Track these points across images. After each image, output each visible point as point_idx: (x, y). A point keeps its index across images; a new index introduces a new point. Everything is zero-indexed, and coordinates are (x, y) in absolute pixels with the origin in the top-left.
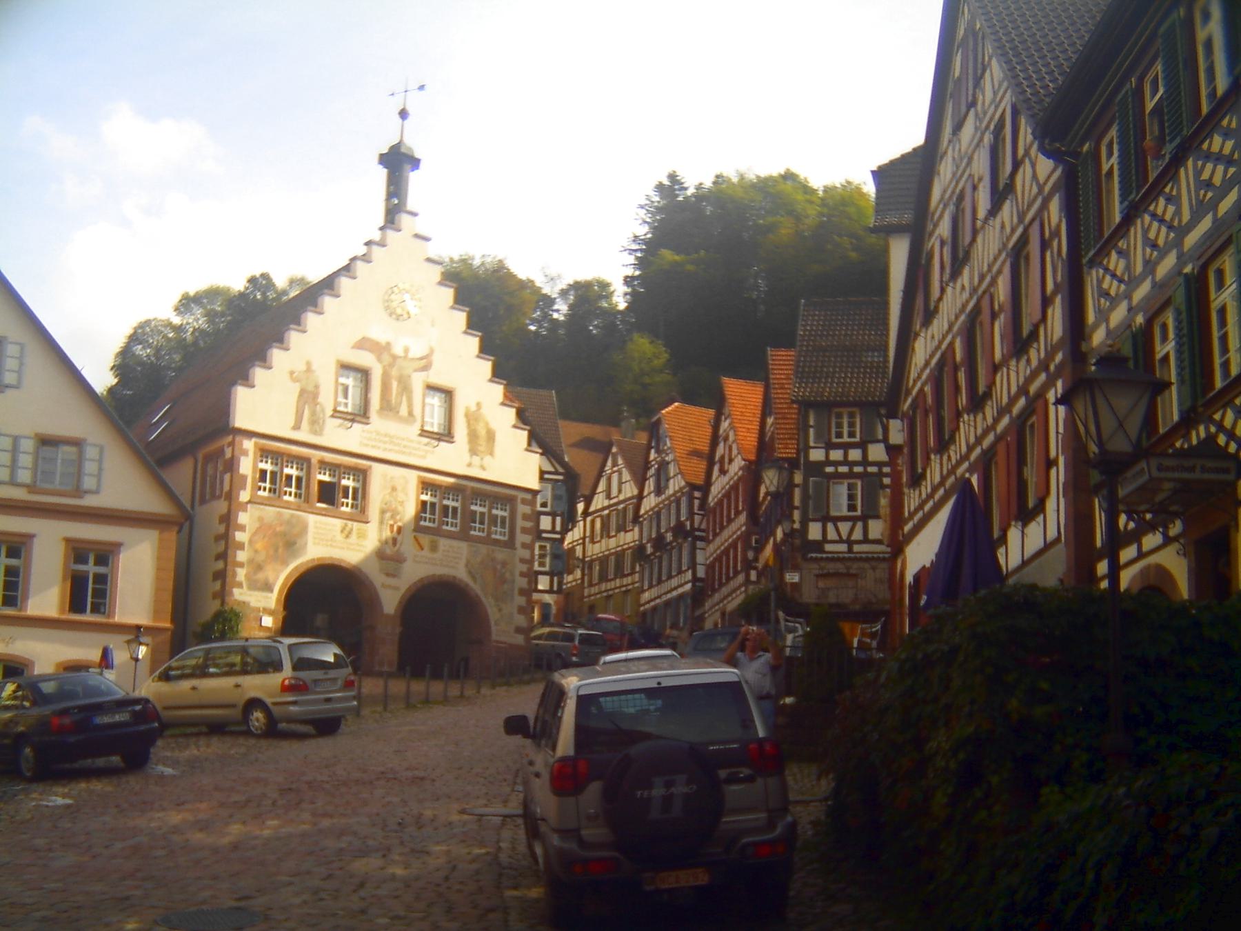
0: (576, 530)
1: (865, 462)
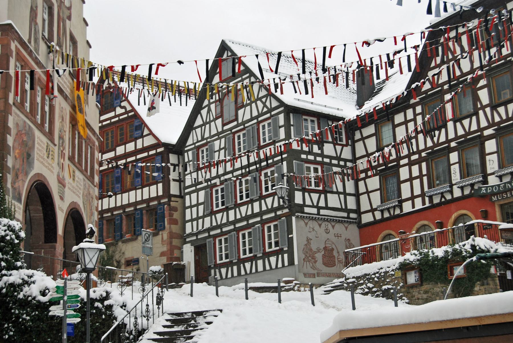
1: (322, 155)
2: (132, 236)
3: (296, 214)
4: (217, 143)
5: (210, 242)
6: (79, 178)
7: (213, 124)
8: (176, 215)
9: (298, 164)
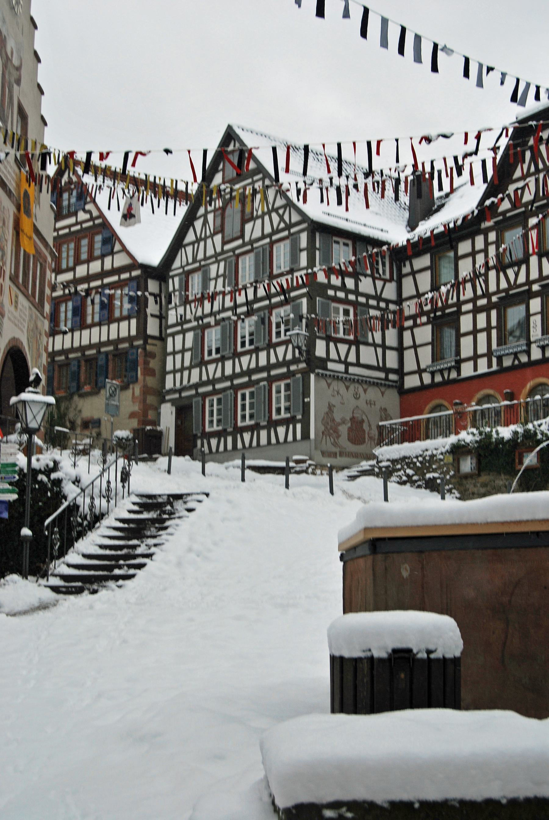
1: (356, 292)
2: (92, 388)
3: (317, 371)
4: (213, 269)
5: (197, 402)
6: (23, 306)
7: (209, 241)
8: (154, 364)
9: (322, 304)
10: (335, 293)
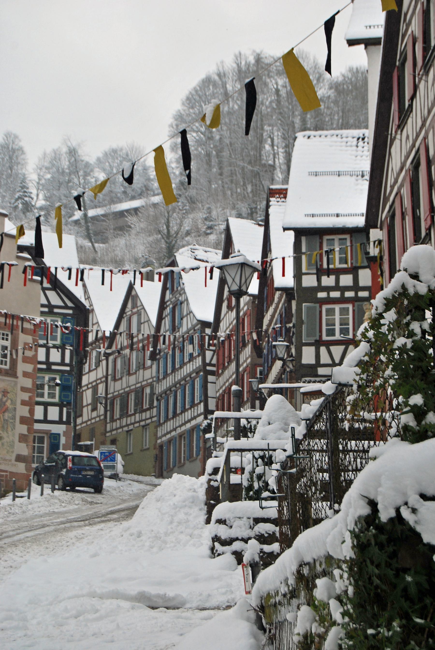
0: (100, 369)
1: (356, 287)
10: (328, 294)
